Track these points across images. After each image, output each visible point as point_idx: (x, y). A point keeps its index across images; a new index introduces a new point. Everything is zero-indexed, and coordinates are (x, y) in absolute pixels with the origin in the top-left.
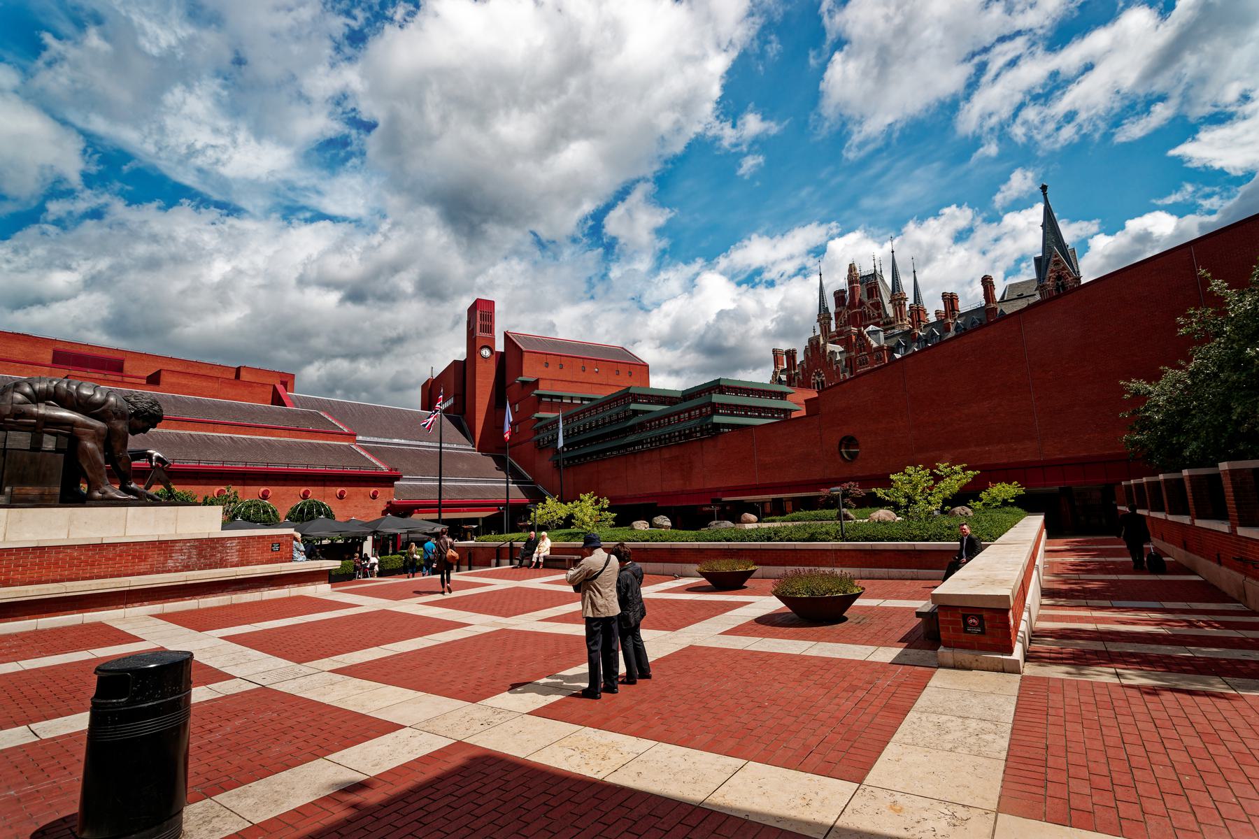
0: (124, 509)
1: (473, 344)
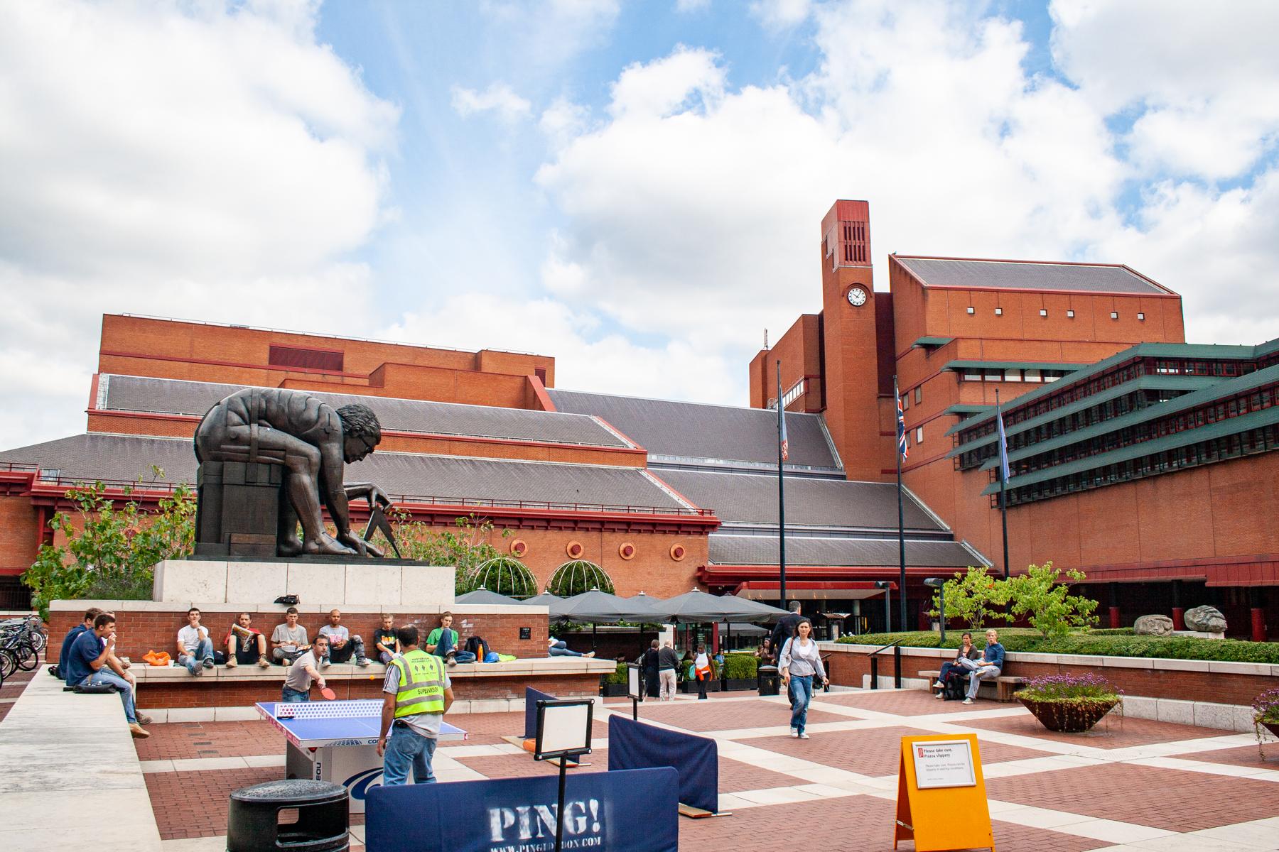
0: (342, 566)
1: (834, 287)
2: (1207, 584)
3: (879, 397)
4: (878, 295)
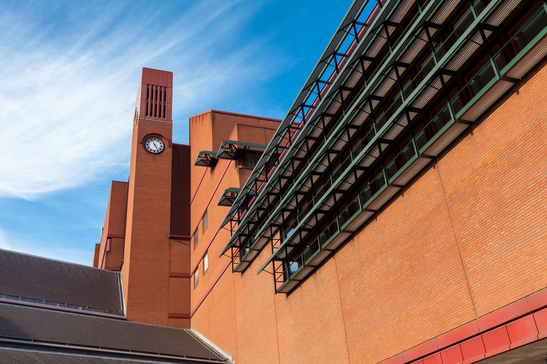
3: (170, 238)
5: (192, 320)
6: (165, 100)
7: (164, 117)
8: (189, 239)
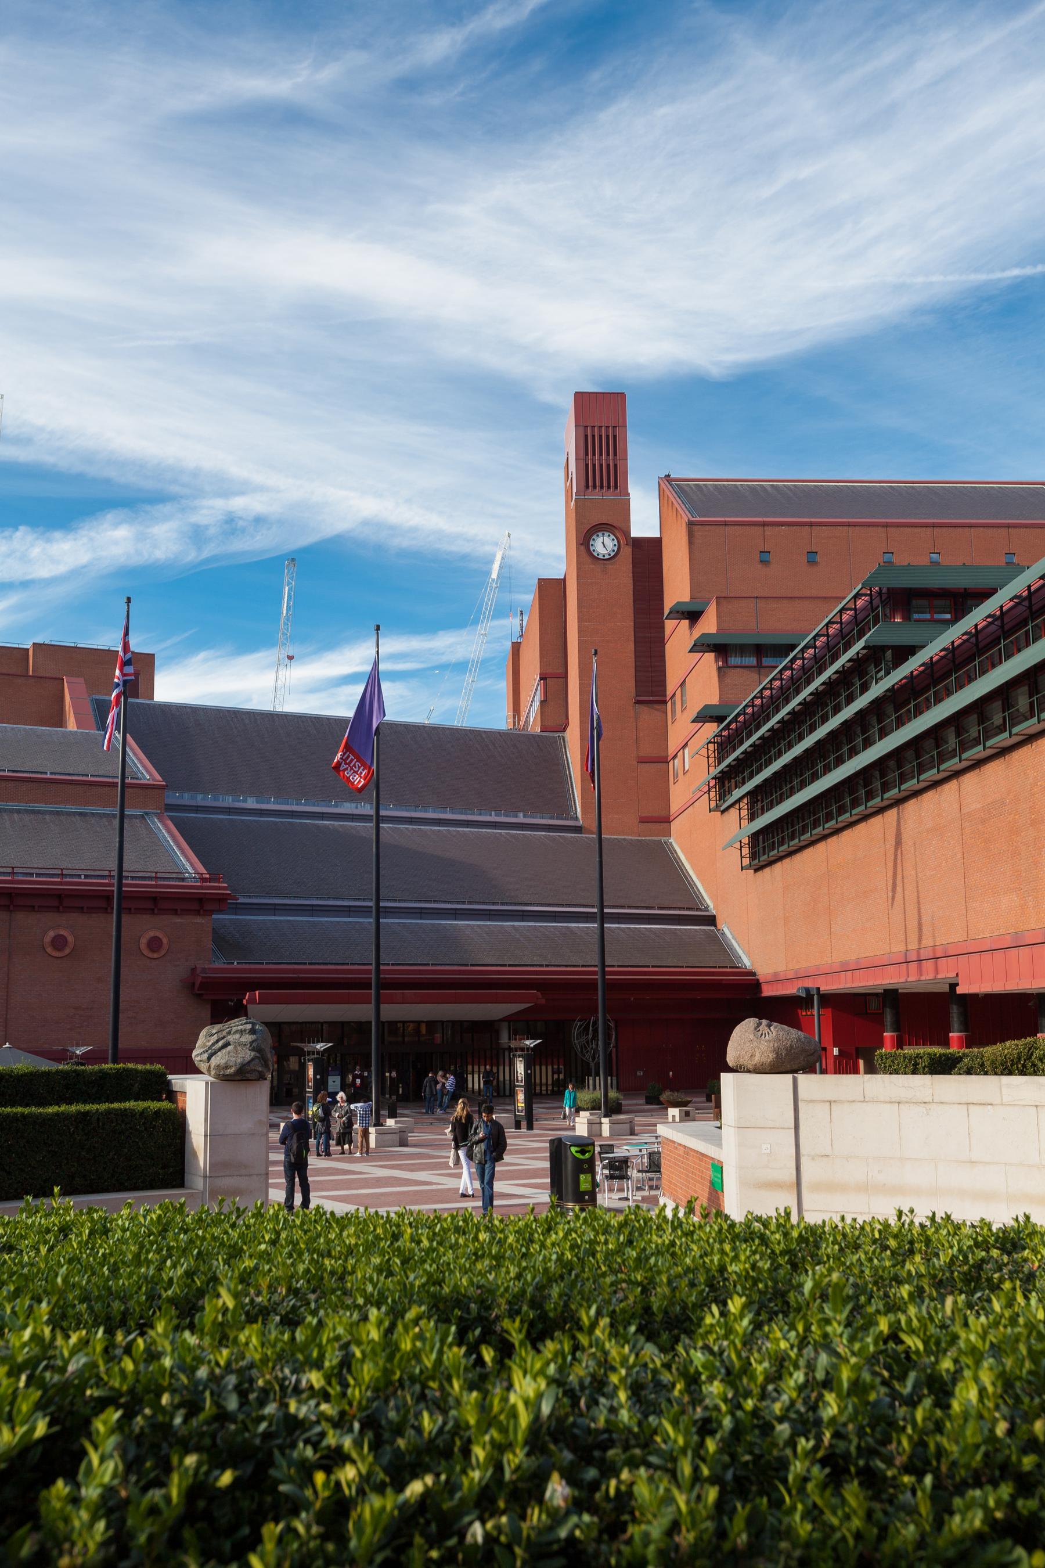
2: (960, 990)
4: (639, 544)
5: (674, 825)
6: (615, 454)
7: (616, 487)
8: (665, 702)
